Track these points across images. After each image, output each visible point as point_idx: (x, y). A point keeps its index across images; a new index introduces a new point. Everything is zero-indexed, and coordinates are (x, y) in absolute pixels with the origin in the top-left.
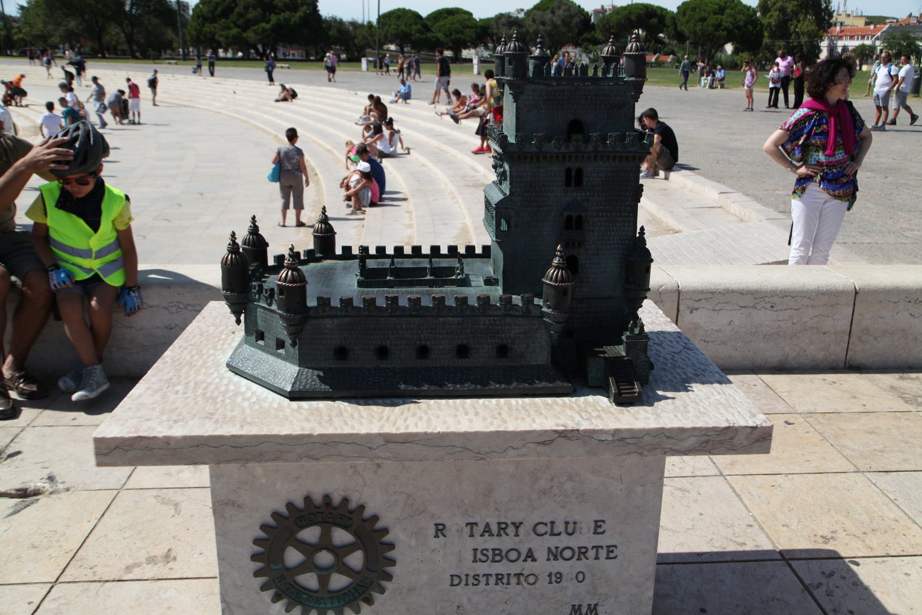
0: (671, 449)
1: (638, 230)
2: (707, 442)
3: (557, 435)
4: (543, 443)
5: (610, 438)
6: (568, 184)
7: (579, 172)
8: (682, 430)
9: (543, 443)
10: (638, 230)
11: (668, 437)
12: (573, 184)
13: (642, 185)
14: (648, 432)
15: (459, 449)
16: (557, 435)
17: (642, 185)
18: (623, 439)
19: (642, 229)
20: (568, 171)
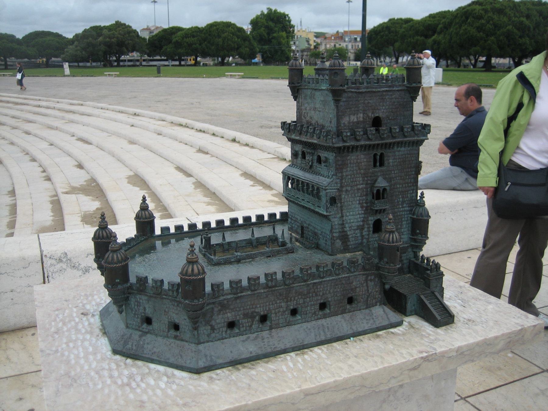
0: (490, 353)
1: (419, 194)
2: (510, 342)
3: (422, 360)
4: (414, 369)
5: (454, 354)
6: (375, 166)
7: (382, 155)
8: (496, 338)
9: (414, 369)
10: (419, 194)
11: (488, 345)
12: (378, 164)
13: (421, 162)
14: (477, 344)
15: (358, 388)
16: (422, 360)
17: (421, 162)
18: (462, 353)
19: (422, 194)
20: (375, 155)
